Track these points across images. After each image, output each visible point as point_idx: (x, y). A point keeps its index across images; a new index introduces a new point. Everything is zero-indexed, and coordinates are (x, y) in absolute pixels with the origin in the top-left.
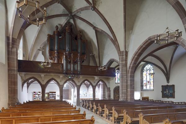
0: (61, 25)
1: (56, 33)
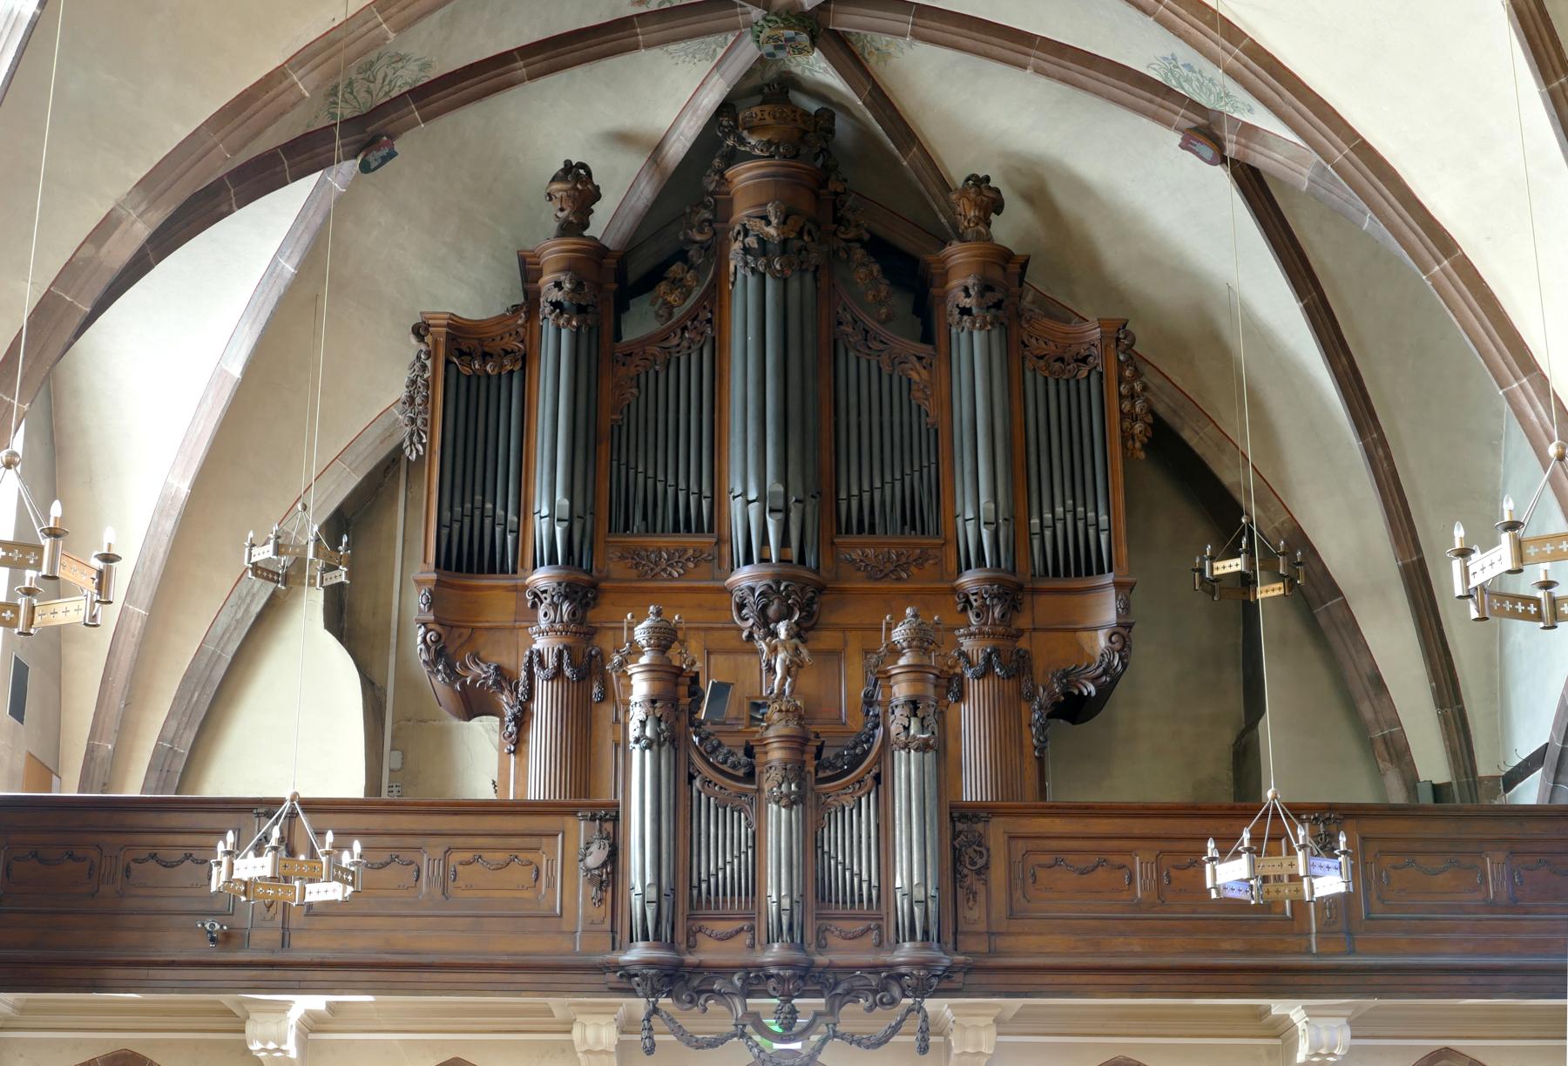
1: (547, 280)
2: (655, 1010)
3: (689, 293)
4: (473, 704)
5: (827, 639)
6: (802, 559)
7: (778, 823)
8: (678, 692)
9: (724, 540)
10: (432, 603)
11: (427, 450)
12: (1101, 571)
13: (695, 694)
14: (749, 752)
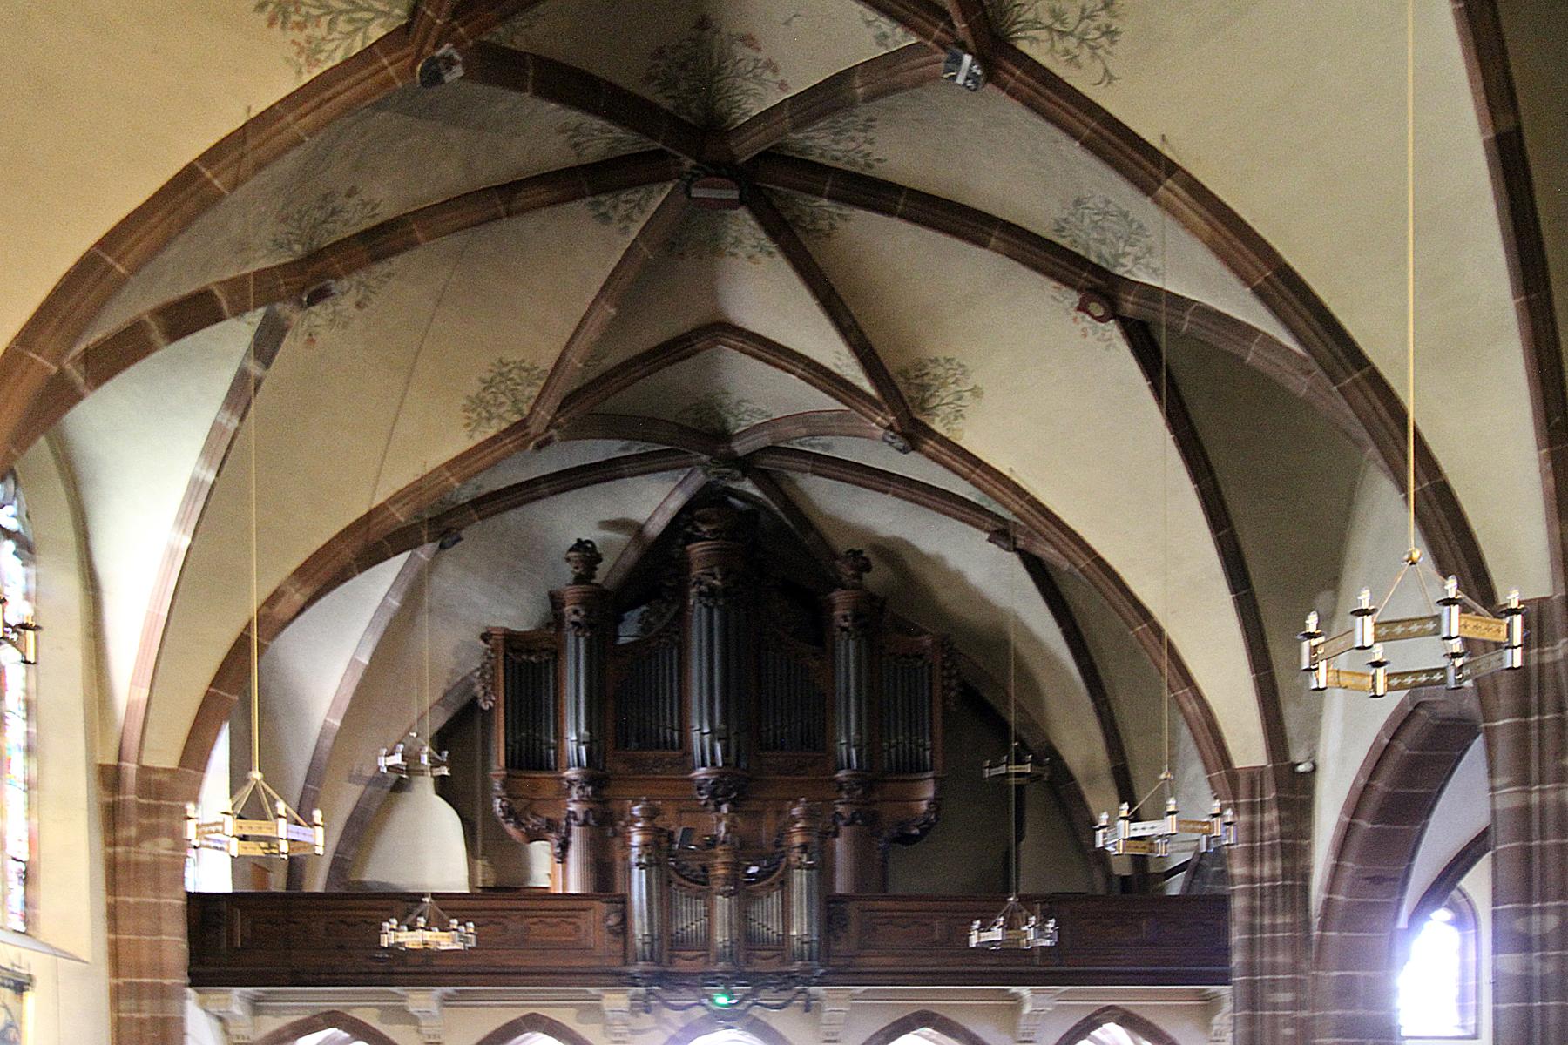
0: (638, 529)
1: (568, 609)
2: (650, 993)
3: (663, 615)
4: (534, 836)
5: (754, 805)
6: (738, 765)
7: (722, 905)
8: (659, 842)
9: (688, 753)
10: (504, 787)
11: (492, 701)
12: (925, 771)
13: (671, 841)
14: (705, 869)
